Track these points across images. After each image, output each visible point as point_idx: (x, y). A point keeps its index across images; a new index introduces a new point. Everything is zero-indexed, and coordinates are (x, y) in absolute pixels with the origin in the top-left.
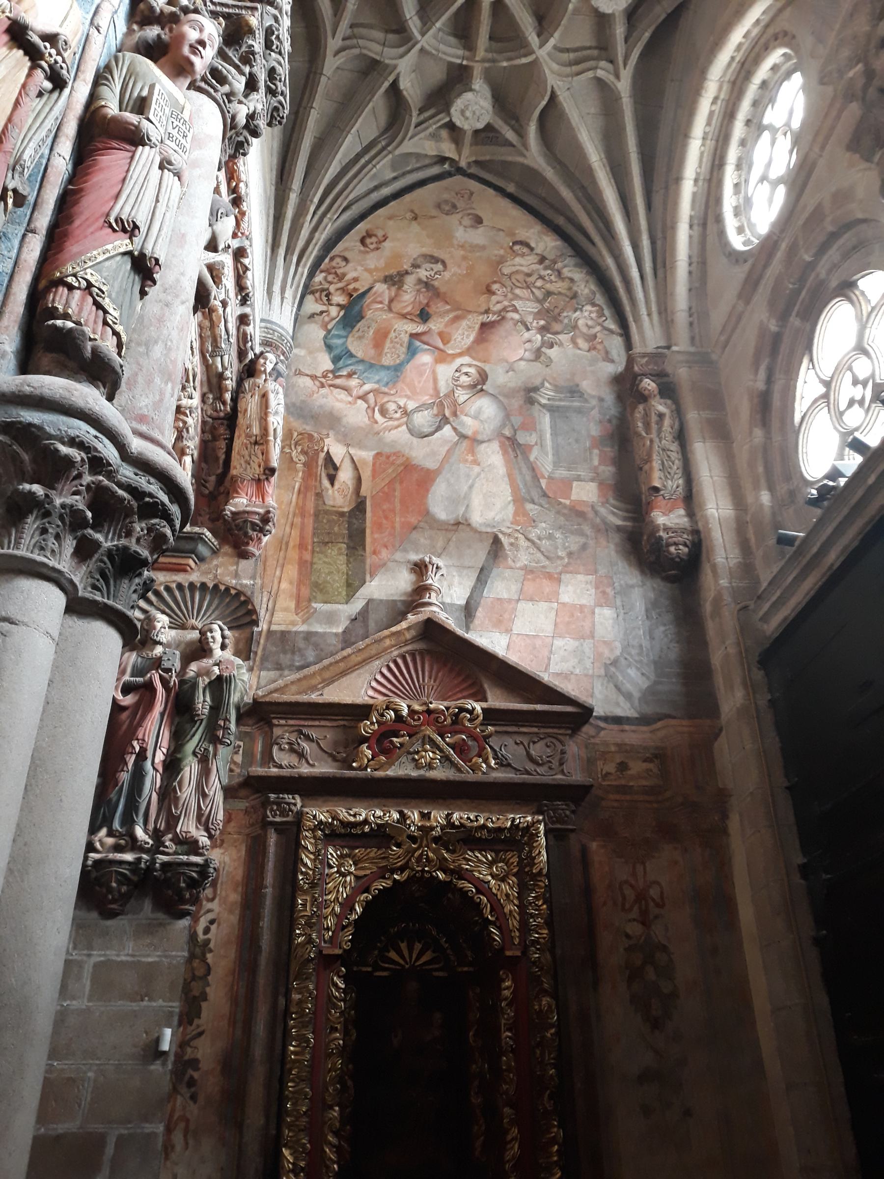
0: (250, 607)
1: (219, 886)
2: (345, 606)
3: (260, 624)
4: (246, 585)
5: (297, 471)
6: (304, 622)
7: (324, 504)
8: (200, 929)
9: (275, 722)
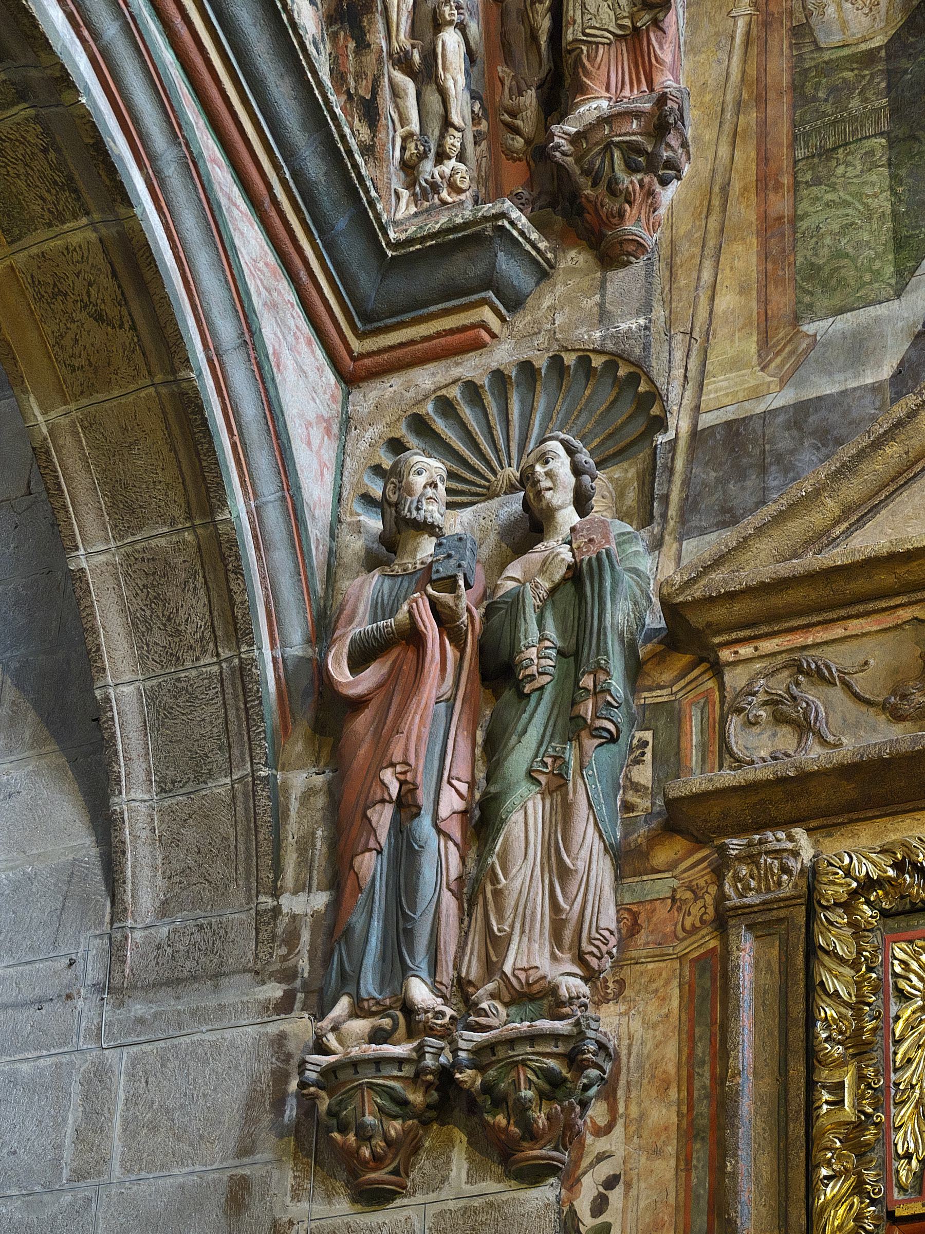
1: (620, 1093)
3: (672, 421)
4: (628, 334)
6: (783, 383)
7: (819, 49)
8: (583, 1207)
9: (726, 655)
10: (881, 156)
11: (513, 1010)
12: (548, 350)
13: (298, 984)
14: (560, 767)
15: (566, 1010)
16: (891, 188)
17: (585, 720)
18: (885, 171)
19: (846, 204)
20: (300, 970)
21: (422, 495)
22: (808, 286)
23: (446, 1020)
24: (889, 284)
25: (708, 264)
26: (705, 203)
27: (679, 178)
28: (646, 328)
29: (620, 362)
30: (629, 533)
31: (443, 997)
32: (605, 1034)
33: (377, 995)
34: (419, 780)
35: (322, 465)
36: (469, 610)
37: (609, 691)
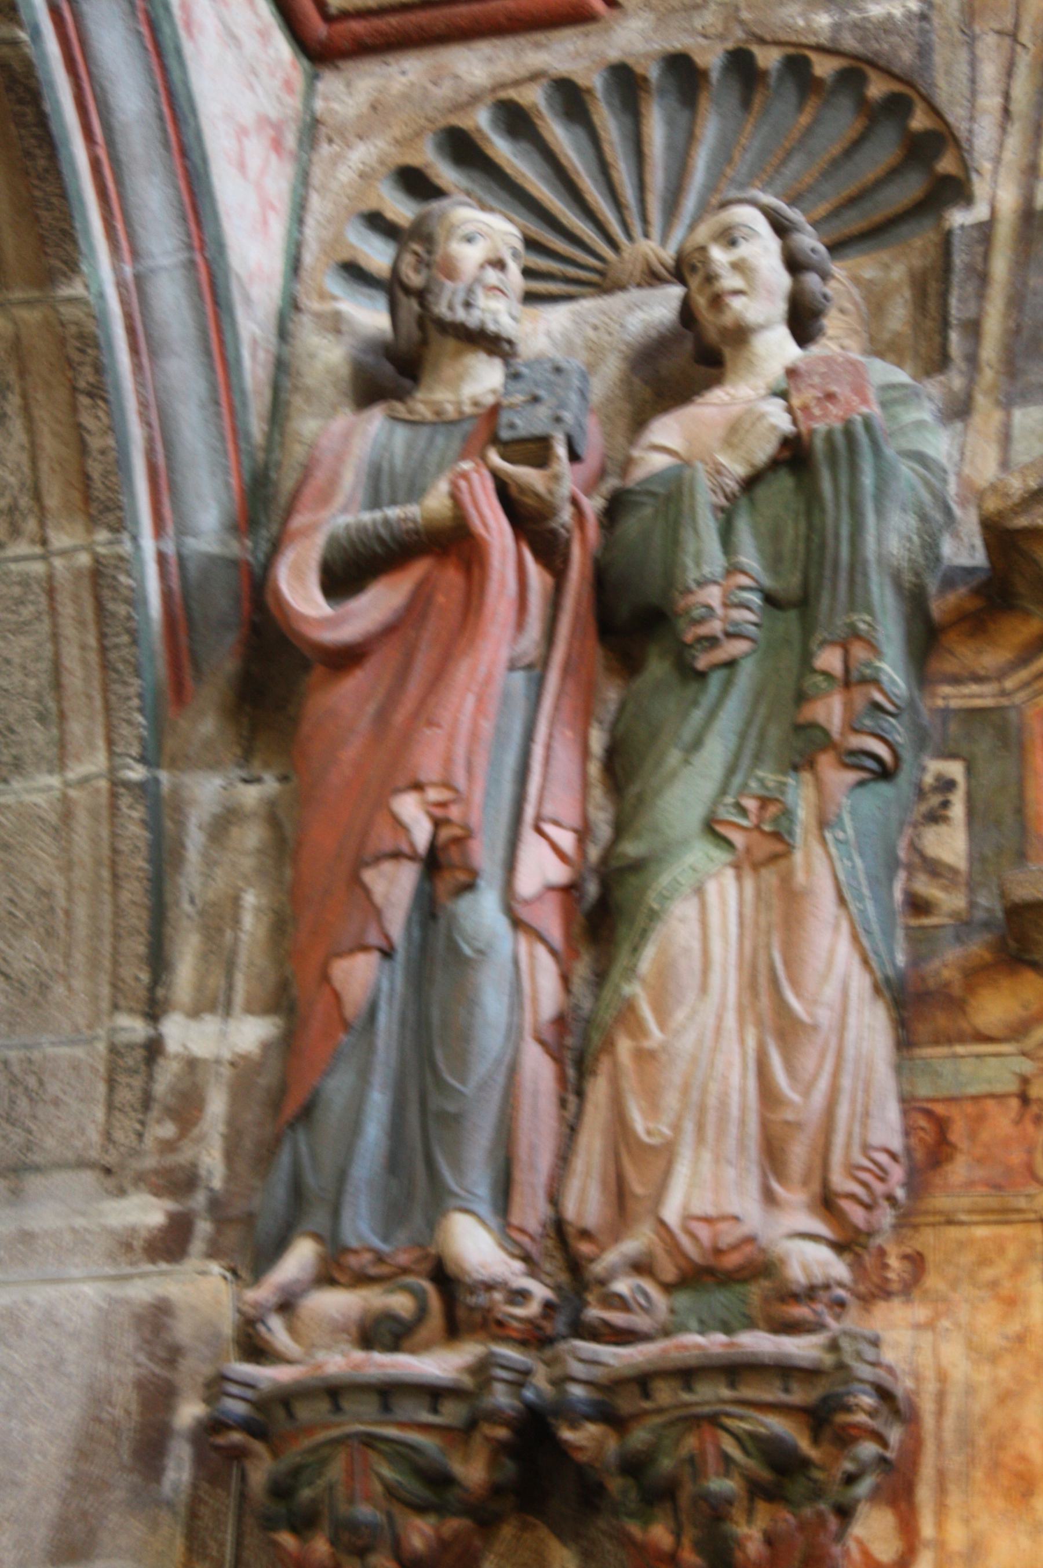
0: (919, 121)
1: (924, 1494)
3: (980, 187)
11: (683, 1300)
12: (722, 37)
13: (199, 1200)
14: (775, 820)
15: (801, 1312)
17: (826, 733)
20: (203, 1172)
21: (478, 280)
23: (532, 1309)
28: (923, 17)
29: (872, 74)
30: (903, 386)
31: (526, 1258)
32: (890, 1370)
33: (377, 1243)
34: (474, 820)
35: (266, 205)
36: (575, 502)
37: (875, 682)
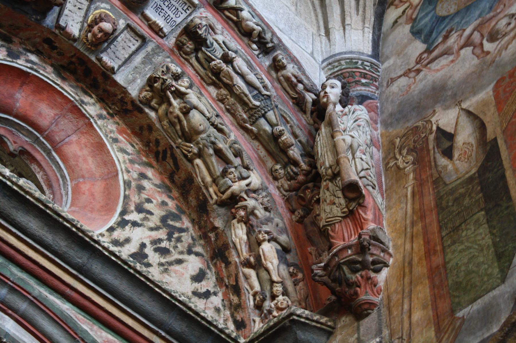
2: (502, 287)
5: (407, 175)
7: (446, 184)
10: (483, 220)
16: (490, 232)
18: (486, 226)
19: (469, 248)
22: (455, 294)
24: (498, 278)
25: (406, 301)
26: (402, 273)
27: (387, 266)
